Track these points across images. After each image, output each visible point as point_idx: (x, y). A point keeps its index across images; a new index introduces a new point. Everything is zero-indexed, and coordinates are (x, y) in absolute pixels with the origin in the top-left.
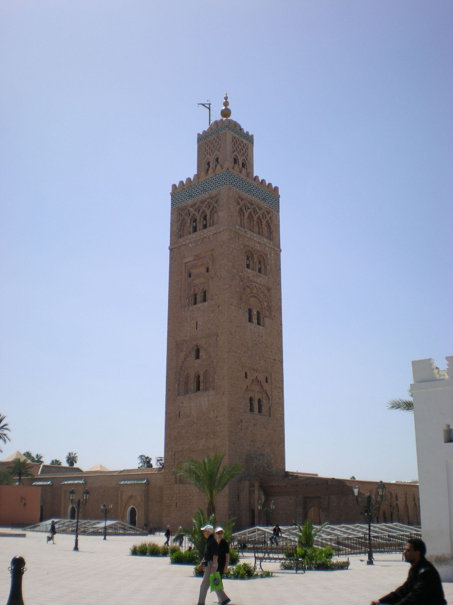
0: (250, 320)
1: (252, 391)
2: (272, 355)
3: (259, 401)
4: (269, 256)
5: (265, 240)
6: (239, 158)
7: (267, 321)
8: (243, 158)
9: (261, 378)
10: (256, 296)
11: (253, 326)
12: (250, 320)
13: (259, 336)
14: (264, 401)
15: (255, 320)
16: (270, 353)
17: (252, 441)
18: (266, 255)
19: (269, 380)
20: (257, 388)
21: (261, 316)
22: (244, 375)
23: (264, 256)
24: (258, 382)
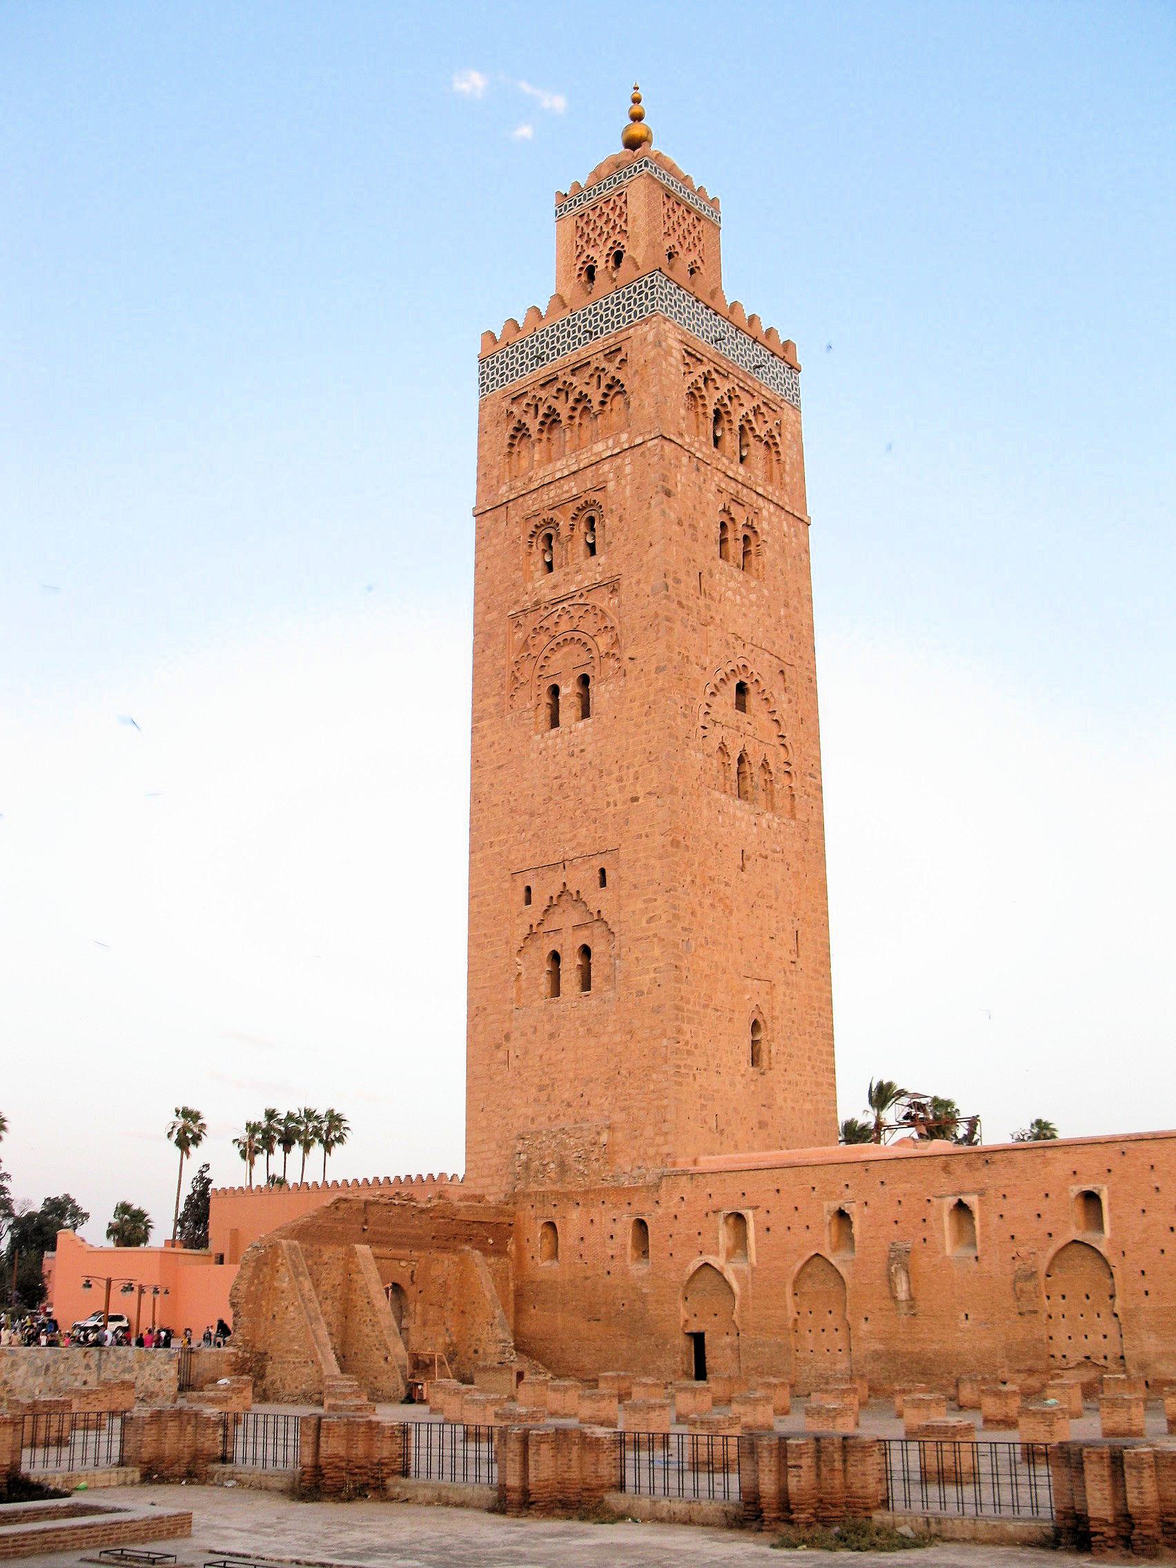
4: (611, 486)
9: (582, 878)
16: (615, 786)
17: (541, 1088)
20: (575, 917)
23: (597, 497)
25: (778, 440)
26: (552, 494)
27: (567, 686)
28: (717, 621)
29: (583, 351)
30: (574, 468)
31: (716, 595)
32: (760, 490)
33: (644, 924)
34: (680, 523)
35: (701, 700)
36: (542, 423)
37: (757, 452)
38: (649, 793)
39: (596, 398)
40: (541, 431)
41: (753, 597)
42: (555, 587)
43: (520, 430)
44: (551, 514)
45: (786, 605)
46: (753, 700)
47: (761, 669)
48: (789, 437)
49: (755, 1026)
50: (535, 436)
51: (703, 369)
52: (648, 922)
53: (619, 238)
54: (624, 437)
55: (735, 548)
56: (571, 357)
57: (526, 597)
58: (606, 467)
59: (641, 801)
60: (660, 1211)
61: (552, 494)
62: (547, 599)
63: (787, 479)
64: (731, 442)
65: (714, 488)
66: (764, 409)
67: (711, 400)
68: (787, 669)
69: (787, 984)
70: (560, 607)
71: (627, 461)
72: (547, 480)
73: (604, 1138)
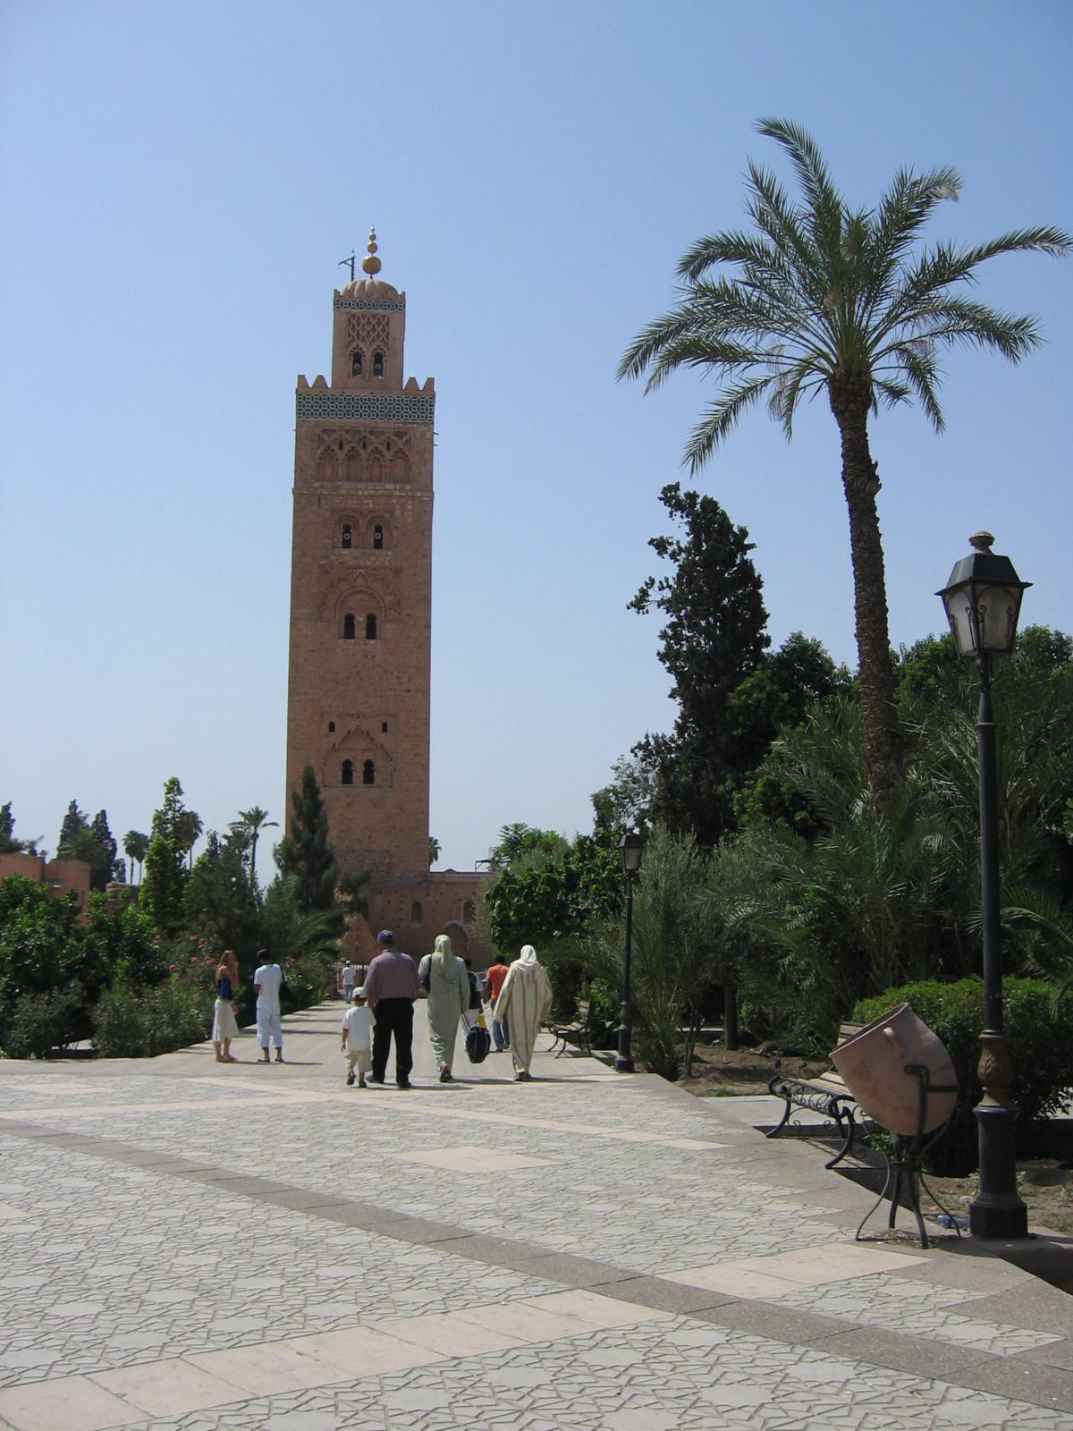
0: (349, 633)
1: (351, 750)
2: (400, 684)
3: (369, 767)
4: (398, 513)
5: (390, 486)
6: (365, 349)
7: (384, 629)
8: (375, 346)
9: (372, 725)
10: (365, 589)
11: (360, 642)
12: (349, 633)
13: (366, 657)
14: (379, 764)
15: (360, 632)
18: (392, 513)
19: (390, 728)
21: (378, 622)
22: (326, 726)
23: (387, 515)
24: (362, 733)
26: (355, 502)
27: (361, 617)
29: (381, 424)
30: (373, 492)
33: (412, 756)
36: (346, 455)
38: (418, 690)
39: (388, 456)
40: (344, 459)
42: (355, 558)
43: (328, 452)
44: (353, 514)
50: (340, 461)
52: (415, 755)
53: (382, 345)
54: (408, 487)
56: (370, 422)
57: (334, 557)
58: (394, 501)
59: (413, 692)
60: (430, 898)
61: (355, 502)
62: (350, 563)
70: (358, 571)
71: (410, 502)
72: (352, 492)
73: (387, 860)
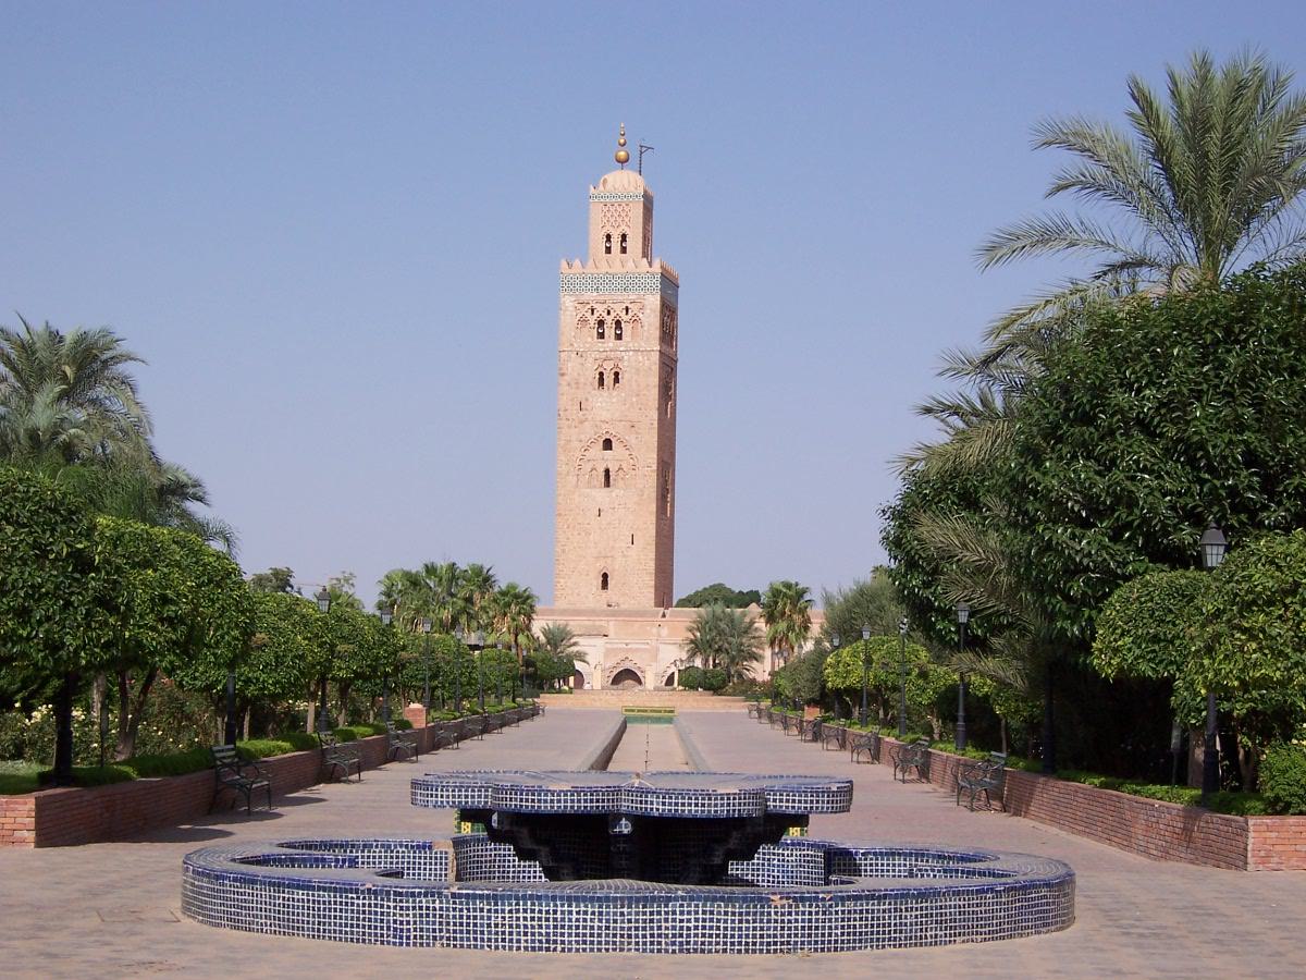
25: (641, 316)
28: (590, 418)
31: (589, 408)
32: (621, 349)
34: (569, 385)
35: (578, 454)
37: (627, 329)
41: (614, 400)
45: (638, 395)
46: (613, 445)
47: (614, 431)
48: (648, 311)
49: (605, 576)
51: (589, 306)
55: (609, 379)
63: (645, 334)
64: (610, 331)
65: (591, 360)
66: (630, 306)
67: (593, 320)
68: (636, 425)
69: (624, 556)
